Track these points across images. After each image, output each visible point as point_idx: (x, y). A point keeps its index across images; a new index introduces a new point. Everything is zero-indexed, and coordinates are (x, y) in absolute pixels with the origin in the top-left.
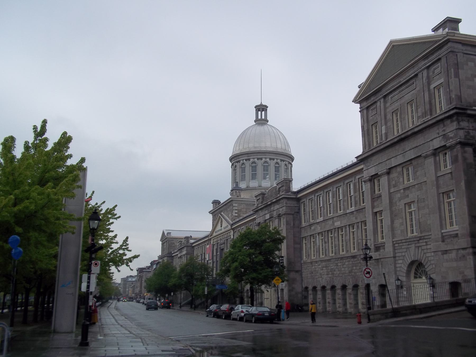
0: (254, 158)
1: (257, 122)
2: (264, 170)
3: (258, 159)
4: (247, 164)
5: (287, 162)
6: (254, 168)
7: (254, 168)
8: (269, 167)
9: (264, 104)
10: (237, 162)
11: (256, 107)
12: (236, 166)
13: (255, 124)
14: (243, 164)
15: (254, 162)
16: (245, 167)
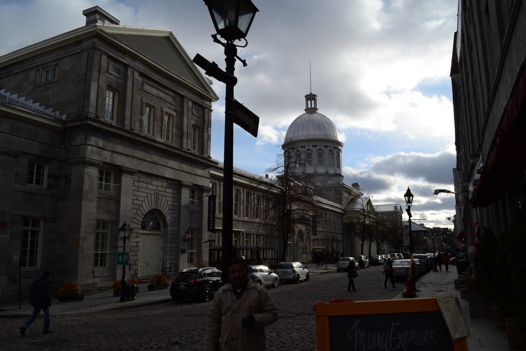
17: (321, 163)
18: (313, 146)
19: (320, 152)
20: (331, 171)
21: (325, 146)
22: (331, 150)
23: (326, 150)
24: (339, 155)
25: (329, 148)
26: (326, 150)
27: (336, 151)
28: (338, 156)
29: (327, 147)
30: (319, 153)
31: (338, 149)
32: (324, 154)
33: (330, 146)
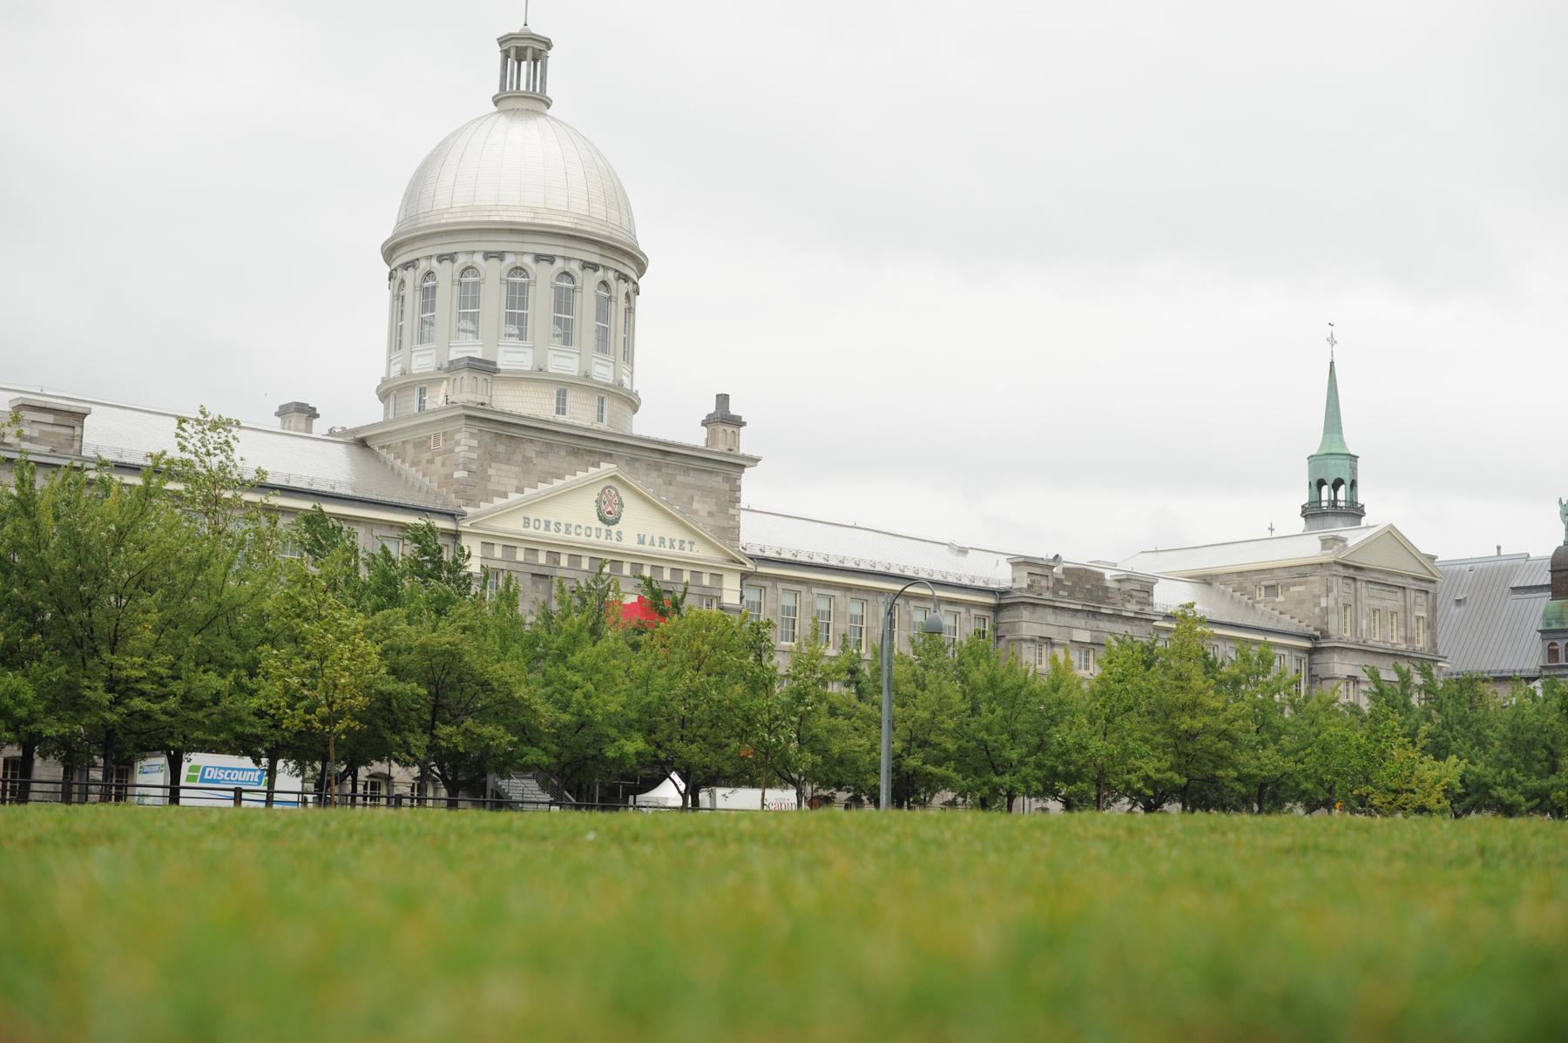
0: (474, 252)
1: (506, 105)
2: (511, 303)
3: (487, 255)
4: (445, 272)
5: (611, 276)
6: (517, 296)
7: (517, 296)
8: (531, 289)
9: (537, 29)
10: (406, 266)
11: (502, 41)
12: (403, 282)
13: (495, 109)
14: (430, 274)
15: (468, 269)
16: (434, 288)
17: (565, 333)
18: (539, 258)
19: (564, 284)
20: (603, 372)
21: (586, 265)
22: (604, 283)
23: (589, 281)
24: (630, 309)
25: (600, 273)
26: (589, 281)
27: (624, 287)
28: (630, 310)
29: (595, 267)
30: (558, 290)
31: (631, 284)
32: (578, 295)
33: (604, 267)
